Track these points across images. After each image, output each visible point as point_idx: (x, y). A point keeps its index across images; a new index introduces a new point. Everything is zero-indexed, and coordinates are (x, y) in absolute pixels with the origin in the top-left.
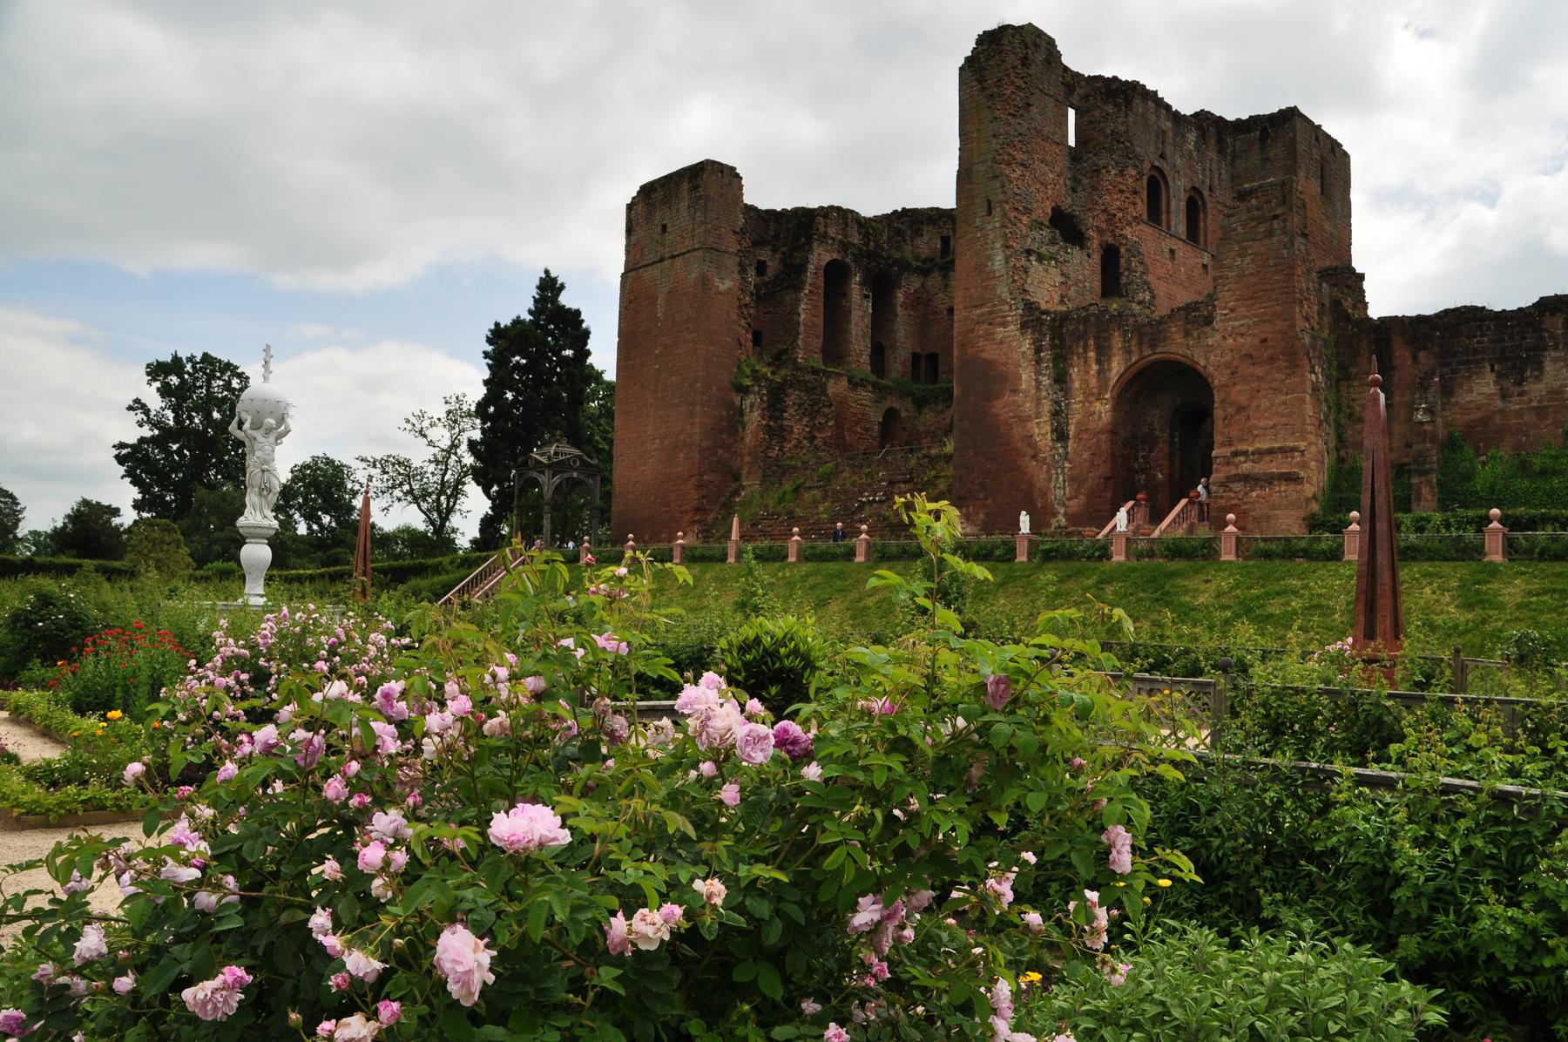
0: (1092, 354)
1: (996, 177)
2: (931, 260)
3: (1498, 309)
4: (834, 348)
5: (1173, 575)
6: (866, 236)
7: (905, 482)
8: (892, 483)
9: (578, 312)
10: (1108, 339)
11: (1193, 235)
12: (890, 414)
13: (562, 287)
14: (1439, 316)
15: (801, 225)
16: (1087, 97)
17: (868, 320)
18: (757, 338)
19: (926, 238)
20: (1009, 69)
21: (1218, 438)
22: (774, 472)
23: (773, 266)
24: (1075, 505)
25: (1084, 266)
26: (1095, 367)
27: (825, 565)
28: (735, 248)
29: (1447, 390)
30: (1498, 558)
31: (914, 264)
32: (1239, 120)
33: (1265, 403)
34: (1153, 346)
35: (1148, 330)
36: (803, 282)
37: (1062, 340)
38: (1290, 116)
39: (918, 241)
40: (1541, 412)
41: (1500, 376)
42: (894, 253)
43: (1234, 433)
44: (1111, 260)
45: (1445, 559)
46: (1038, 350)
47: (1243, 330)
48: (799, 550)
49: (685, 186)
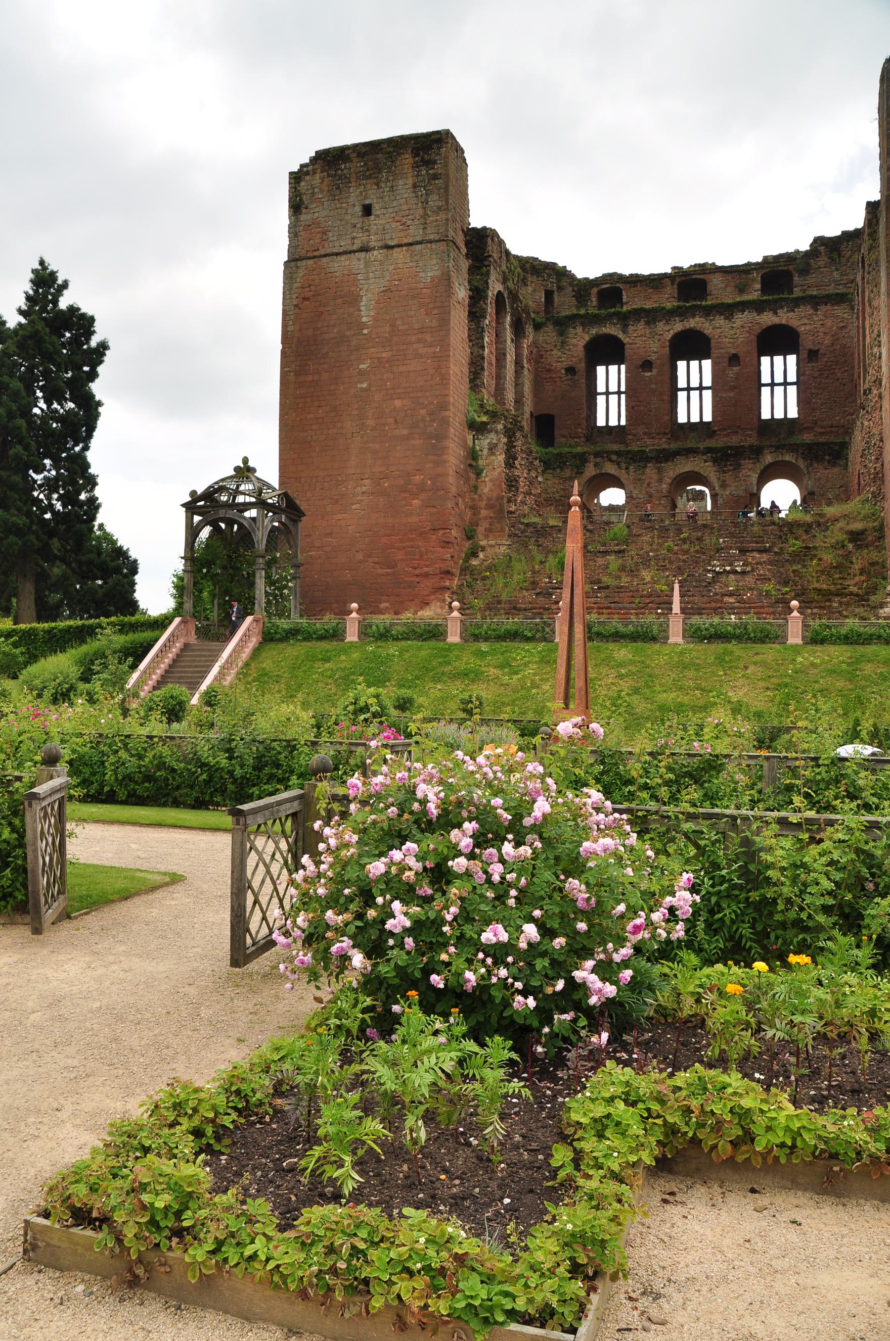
7: (760, 551)
8: (743, 551)
9: (92, 320)
13: (65, 285)
19: (530, 289)
49: (407, 159)
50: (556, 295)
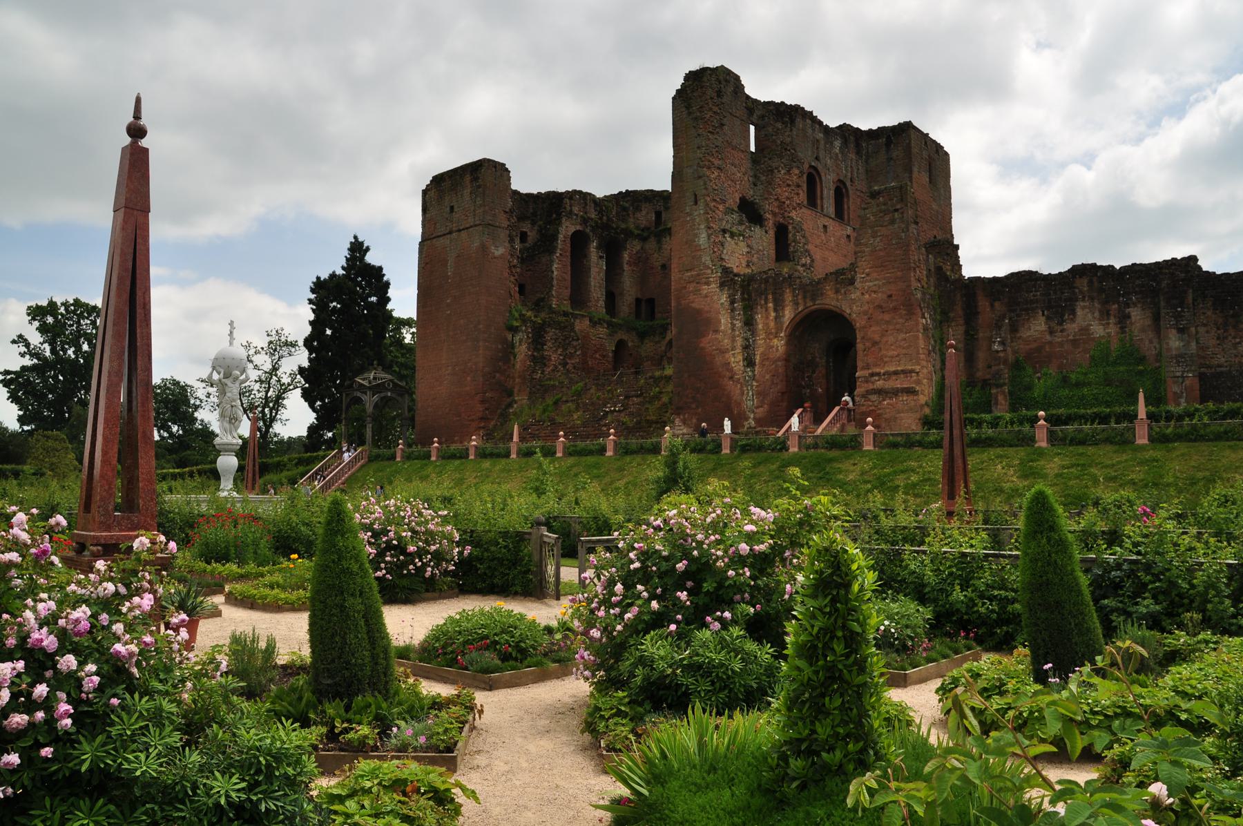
0: (771, 305)
1: (700, 177)
2: (648, 229)
3: (1046, 273)
4: (578, 296)
5: (831, 460)
6: (600, 212)
7: (637, 396)
8: (627, 397)
9: (381, 268)
10: (782, 294)
11: (840, 214)
12: (621, 345)
13: (368, 249)
14: (1007, 277)
15: (552, 205)
16: (762, 117)
17: (602, 275)
18: (522, 289)
19: (644, 213)
20: (708, 100)
21: (860, 364)
22: (539, 390)
23: (532, 235)
24: (761, 412)
25: (763, 239)
26: (773, 314)
27: (584, 459)
28: (505, 223)
29: (1014, 329)
30: (1044, 444)
31: (636, 232)
32: (870, 130)
33: (891, 339)
34: (813, 299)
35: (810, 288)
36: (555, 248)
37: (749, 295)
38: (906, 128)
39: (638, 215)
40: (1075, 343)
41: (1048, 318)
42: (622, 223)
43: (871, 360)
44: (782, 233)
45: (1011, 446)
46: (732, 302)
47: (875, 288)
48: (564, 448)
49: (468, 178)
50: (663, 215)
